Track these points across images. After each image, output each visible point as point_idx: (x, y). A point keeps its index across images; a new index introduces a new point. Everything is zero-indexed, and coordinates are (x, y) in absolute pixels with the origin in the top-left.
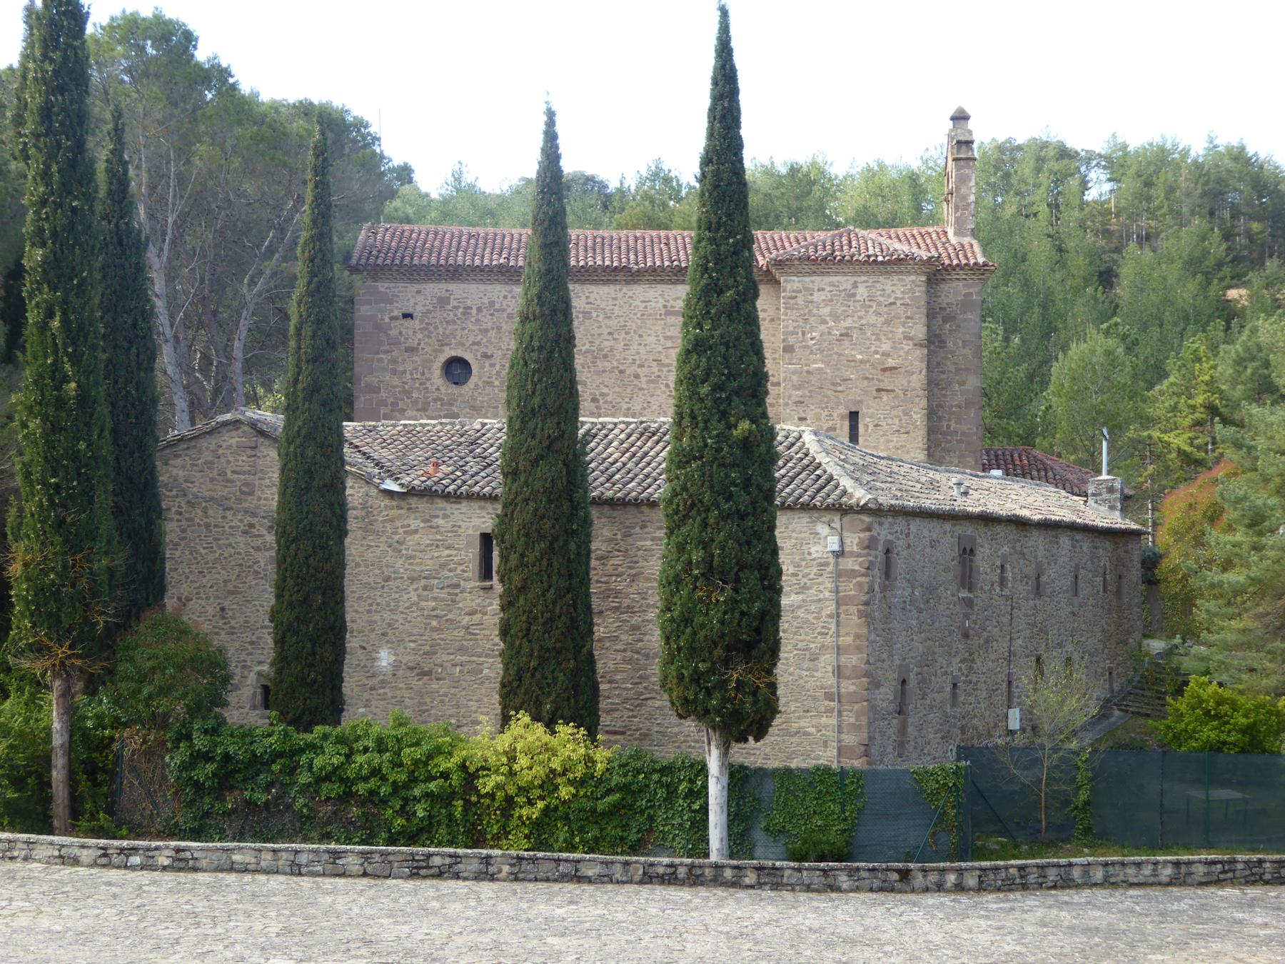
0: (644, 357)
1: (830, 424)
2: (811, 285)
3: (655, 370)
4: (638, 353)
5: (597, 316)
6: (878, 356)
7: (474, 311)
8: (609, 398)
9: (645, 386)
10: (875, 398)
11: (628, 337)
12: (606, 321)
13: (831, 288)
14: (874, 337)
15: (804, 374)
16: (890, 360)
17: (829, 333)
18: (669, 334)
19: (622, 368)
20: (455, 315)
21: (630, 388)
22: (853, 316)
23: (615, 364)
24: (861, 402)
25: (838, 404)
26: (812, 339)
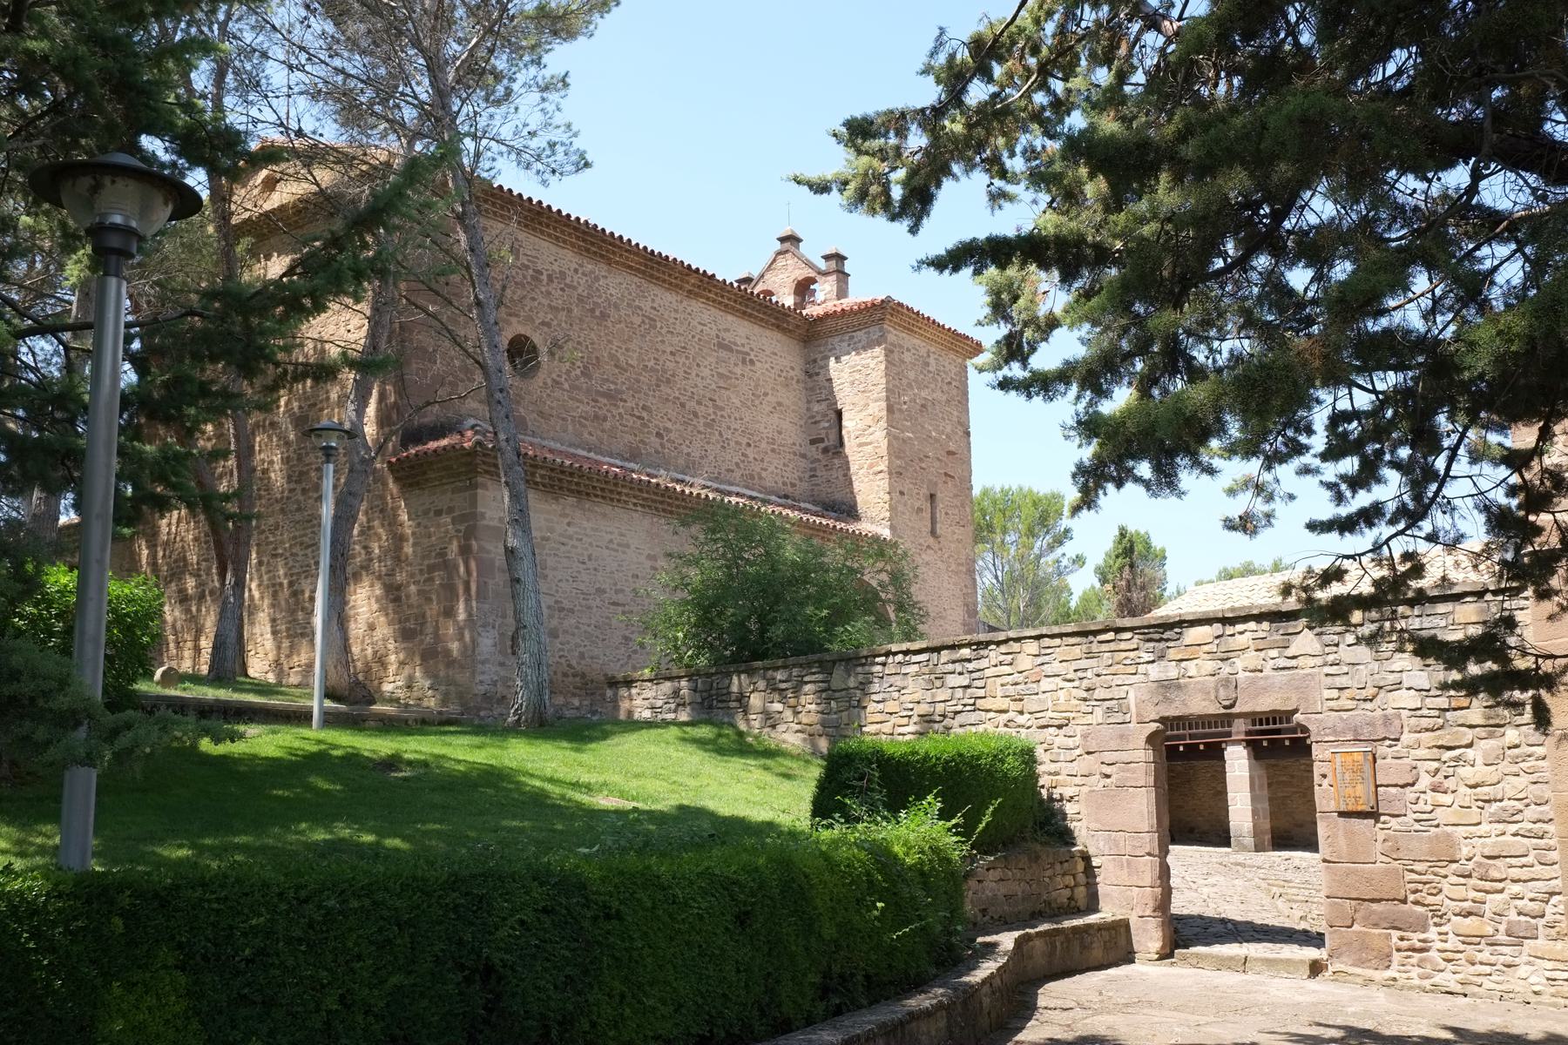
1: (917, 505)
3: (711, 411)
4: (696, 386)
7: (544, 277)
8: (672, 436)
9: (701, 429)
18: (720, 370)
19: (683, 399)
20: (525, 277)
23: (677, 395)
24: (936, 484)
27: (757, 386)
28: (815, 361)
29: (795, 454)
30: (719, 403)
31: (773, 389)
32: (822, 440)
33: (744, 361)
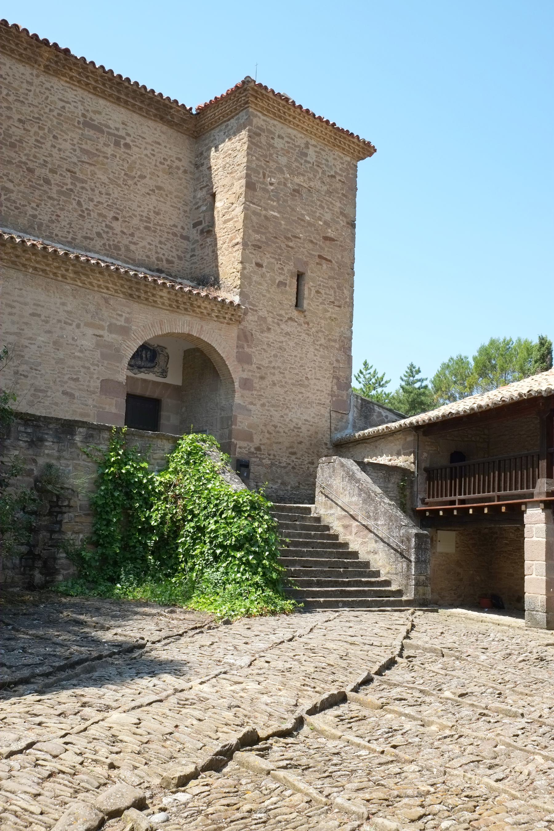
0: (58, 163)
1: (281, 278)
2: (272, 129)
4: (51, 155)
5: (8, 95)
6: (321, 223)
8: (13, 196)
9: (55, 196)
10: (317, 264)
11: (41, 133)
12: (18, 104)
13: (289, 140)
14: (319, 203)
15: (263, 218)
16: (329, 230)
17: (285, 185)
18: (84, 146)
19: (31, 165)
21: (37, 193)
22: (303, 175)
23: (24, 159)
24: (306, 263)
25: (289, 259)
26: (271, 184)
27: (131, 168)
28: (201, 154)
29: (175, 234)
30: (81, 176)
31: (152, 174)
32: (200, 223)
33: (117, 144)
